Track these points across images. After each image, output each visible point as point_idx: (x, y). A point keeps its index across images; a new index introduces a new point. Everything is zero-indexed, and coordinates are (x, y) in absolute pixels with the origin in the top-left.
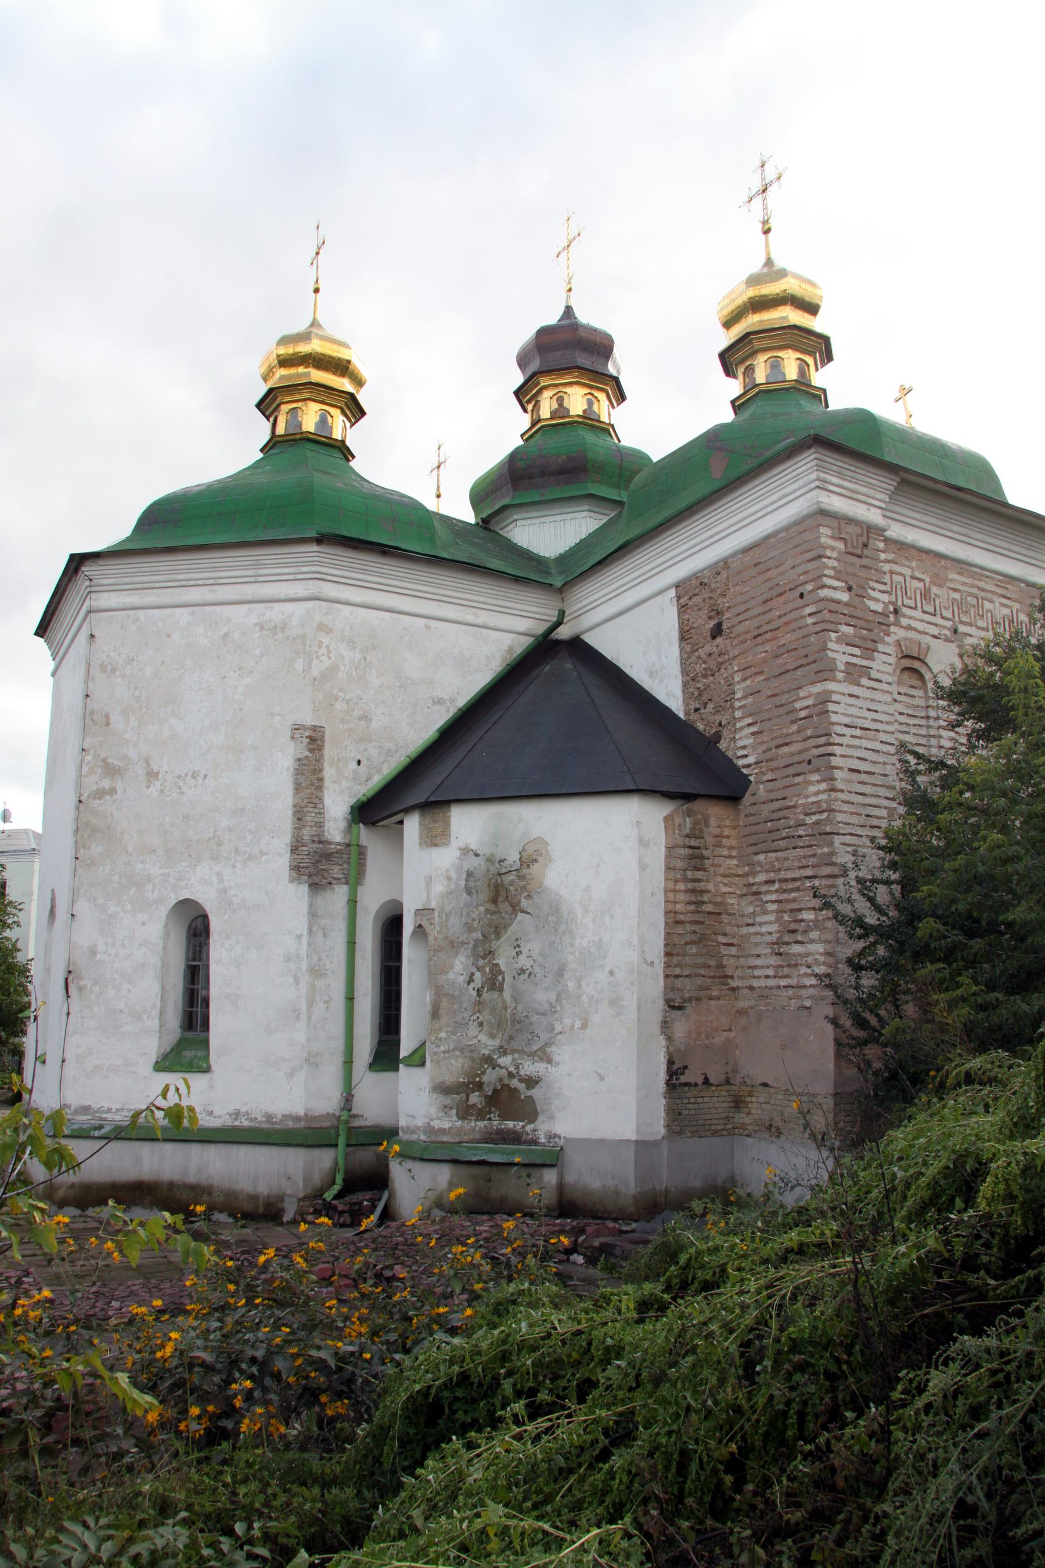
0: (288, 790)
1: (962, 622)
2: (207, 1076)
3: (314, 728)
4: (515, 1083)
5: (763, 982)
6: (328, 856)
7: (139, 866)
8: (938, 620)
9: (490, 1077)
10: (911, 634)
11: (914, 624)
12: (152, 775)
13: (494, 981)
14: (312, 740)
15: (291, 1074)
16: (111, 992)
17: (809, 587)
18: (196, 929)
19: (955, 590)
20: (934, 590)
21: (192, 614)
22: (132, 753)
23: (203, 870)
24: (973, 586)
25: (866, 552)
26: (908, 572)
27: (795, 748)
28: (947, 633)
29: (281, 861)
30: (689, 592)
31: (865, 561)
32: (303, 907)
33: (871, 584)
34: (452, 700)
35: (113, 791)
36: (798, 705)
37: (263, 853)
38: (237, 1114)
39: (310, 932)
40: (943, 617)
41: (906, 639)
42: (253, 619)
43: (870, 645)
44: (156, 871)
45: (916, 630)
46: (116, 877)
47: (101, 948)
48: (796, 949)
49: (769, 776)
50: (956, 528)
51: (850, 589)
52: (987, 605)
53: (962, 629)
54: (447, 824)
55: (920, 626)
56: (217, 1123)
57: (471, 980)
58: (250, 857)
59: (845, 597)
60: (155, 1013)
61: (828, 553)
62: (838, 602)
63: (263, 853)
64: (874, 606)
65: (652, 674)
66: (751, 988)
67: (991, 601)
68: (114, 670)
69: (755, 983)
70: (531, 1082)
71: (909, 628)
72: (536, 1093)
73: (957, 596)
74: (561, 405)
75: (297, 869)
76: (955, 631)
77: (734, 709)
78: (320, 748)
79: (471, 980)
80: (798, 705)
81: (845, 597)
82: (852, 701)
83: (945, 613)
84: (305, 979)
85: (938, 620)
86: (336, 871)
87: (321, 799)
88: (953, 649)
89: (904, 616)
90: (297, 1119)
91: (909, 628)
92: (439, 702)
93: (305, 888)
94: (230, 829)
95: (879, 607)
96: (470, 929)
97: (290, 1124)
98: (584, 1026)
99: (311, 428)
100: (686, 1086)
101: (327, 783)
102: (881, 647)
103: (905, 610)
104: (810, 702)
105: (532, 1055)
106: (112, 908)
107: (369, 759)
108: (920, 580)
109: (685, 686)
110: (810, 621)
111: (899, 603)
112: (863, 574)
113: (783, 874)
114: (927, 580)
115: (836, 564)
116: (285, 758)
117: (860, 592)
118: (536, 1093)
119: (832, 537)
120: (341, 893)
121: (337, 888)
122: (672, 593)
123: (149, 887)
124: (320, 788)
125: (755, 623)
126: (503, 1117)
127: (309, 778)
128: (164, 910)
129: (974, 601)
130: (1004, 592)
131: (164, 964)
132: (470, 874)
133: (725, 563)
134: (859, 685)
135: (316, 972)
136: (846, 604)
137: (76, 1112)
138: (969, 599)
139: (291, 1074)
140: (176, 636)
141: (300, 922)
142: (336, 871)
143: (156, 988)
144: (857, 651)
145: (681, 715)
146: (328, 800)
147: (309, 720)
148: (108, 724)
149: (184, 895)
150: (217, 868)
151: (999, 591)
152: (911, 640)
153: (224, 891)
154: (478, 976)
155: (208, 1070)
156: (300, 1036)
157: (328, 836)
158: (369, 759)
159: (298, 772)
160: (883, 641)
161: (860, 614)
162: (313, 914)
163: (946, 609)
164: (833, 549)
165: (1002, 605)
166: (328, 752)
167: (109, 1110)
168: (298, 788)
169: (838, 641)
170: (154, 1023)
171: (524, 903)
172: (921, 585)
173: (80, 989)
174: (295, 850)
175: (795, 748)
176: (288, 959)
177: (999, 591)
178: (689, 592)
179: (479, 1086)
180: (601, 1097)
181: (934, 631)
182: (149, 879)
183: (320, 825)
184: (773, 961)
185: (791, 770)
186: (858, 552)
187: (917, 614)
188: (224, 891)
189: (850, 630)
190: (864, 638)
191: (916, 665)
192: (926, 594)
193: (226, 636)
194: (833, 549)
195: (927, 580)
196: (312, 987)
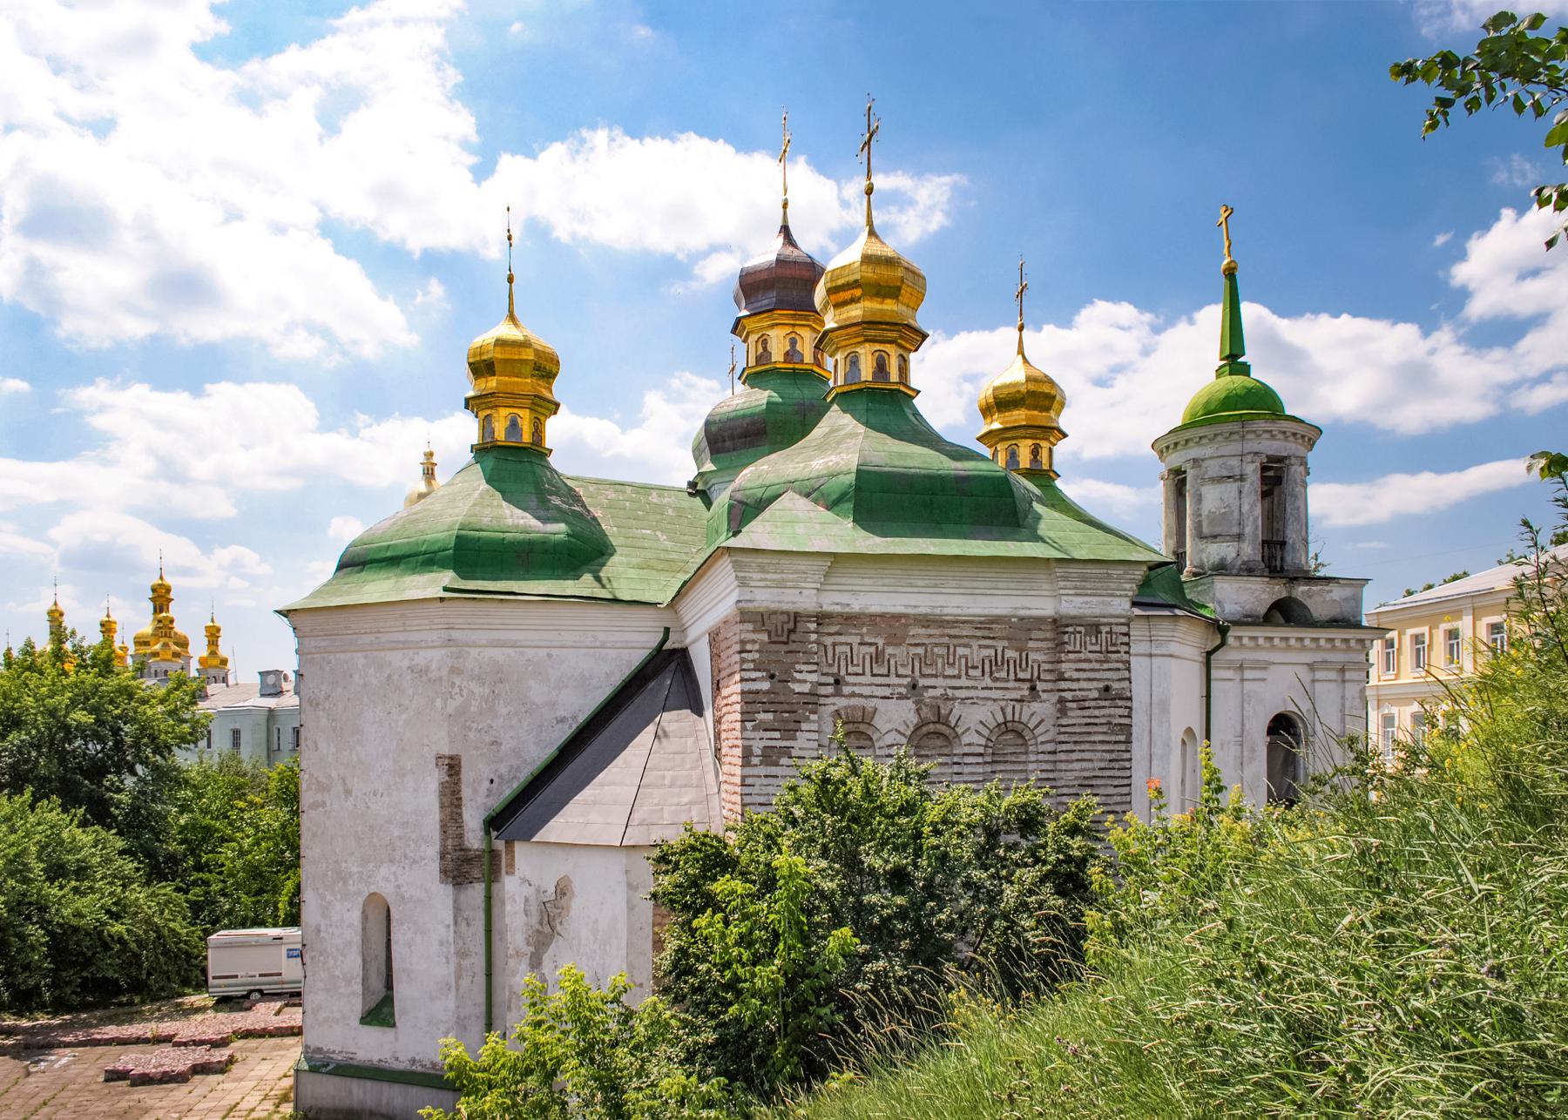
1: (923, 676)
3: (451, 758)
6: (468, 861)
8: (893, 680)
10: (854, 701)
11: (857, 690)
14: (451, 767)
16: (332, 962)
19: (917, 645)
20: (889, 650)
23: (384, 870)
24: (942, 636)
25: (793, 637)
26: (855, 640)
28: (903, 690)
29: (434, 867)
31: (793, 647)
32: (450, 903)
33: (798, 667)
34: (574, 718)
37: (422, 859)
38: (413, 1061)
39: (456, 923)
40: (898, 676)
41: (846, 708)
43: (792, 726)
44: (355, 870)
45: (861, 695)
50: (920, 583)
51: (772, 677)
52: (961, 651)
53: (922, 682)
55: (866, 691)
56: (401, 1066)
58: (414, 862)
59: (765, 686)
60: (359, 979)
61: (748, 647)
62: (757, 692)
63: (422, 859)
64: (797, 688)
67: (966, 646)
71: (853, 695)
73: (920, 650)
75: (444, 871)
76: (914, 687)
78: (458, 773)
81: (766, 686)
82: (771, 780)
83: (901, 671)
84: (453, 959)
85: (893, 680)
86: (476, 873)
87: (460, 815)
88: (910, 704)
89: (847, 684)
91: (853, 695)
92: (562, 720)
93: (450, 888)
94: (400, 838)
95: (806, 688)
96: (528, 944)
101: (465, 801)
102: (804, 726)
103: (849, 679)
106: (329, 898)
107: (501, 777)
108: (871, 644)
111: (843, 672)
112: (789, 659)
114: (881, 642)
115: (757, 656)
116: (433, 781)
117: (784, 677)
119: (754, 631)
120: (476, 892)
121: (476, 885)
124: (459, 806)
127: (451, 797)
128: (361, 900)
129: (943, 651)
130: (986, 633)
131: (365, 940)
132: (527, 900)
134: (777, 764)
135: (462, 954)
136: (767, 692)
138: (936, 650)
141: (448, 916)
142: (476, 873)
143: (359, 961)
144: (777, 735)
146: (466, 816)
147: (446, 752)
149: (373, 889)
150: (393, 869)
151: (979, 633)
152: (854, 708)
153: (399, 887)
155: (394, 1025)
156: (452, 1005)
157: (467, 844)
158: (501, 777)
159: (442, 794)
160: (807, 720)
161: (782, 699)
162: (457, 909)
163: (903, 666)
164: (754, 642)
165: (980, 647)
166: (466, 775)
168: (442, 807)
169: (755, 729)
170: (358, 988)
171: (559, 928)
172: (872, 649)
174: (442, 857)
176: (441, 944)
177: (979, 633)
181: (887, 692)
183: (461, 836)
186: (784, 639)
187: (868, 679)
188: (399, 887)
189: (770, 716)
190: (784, 721)
191: (862, 727)
192: (878, 657)
194: (754, 642)
195: (881, 642)
196: (460, 965)
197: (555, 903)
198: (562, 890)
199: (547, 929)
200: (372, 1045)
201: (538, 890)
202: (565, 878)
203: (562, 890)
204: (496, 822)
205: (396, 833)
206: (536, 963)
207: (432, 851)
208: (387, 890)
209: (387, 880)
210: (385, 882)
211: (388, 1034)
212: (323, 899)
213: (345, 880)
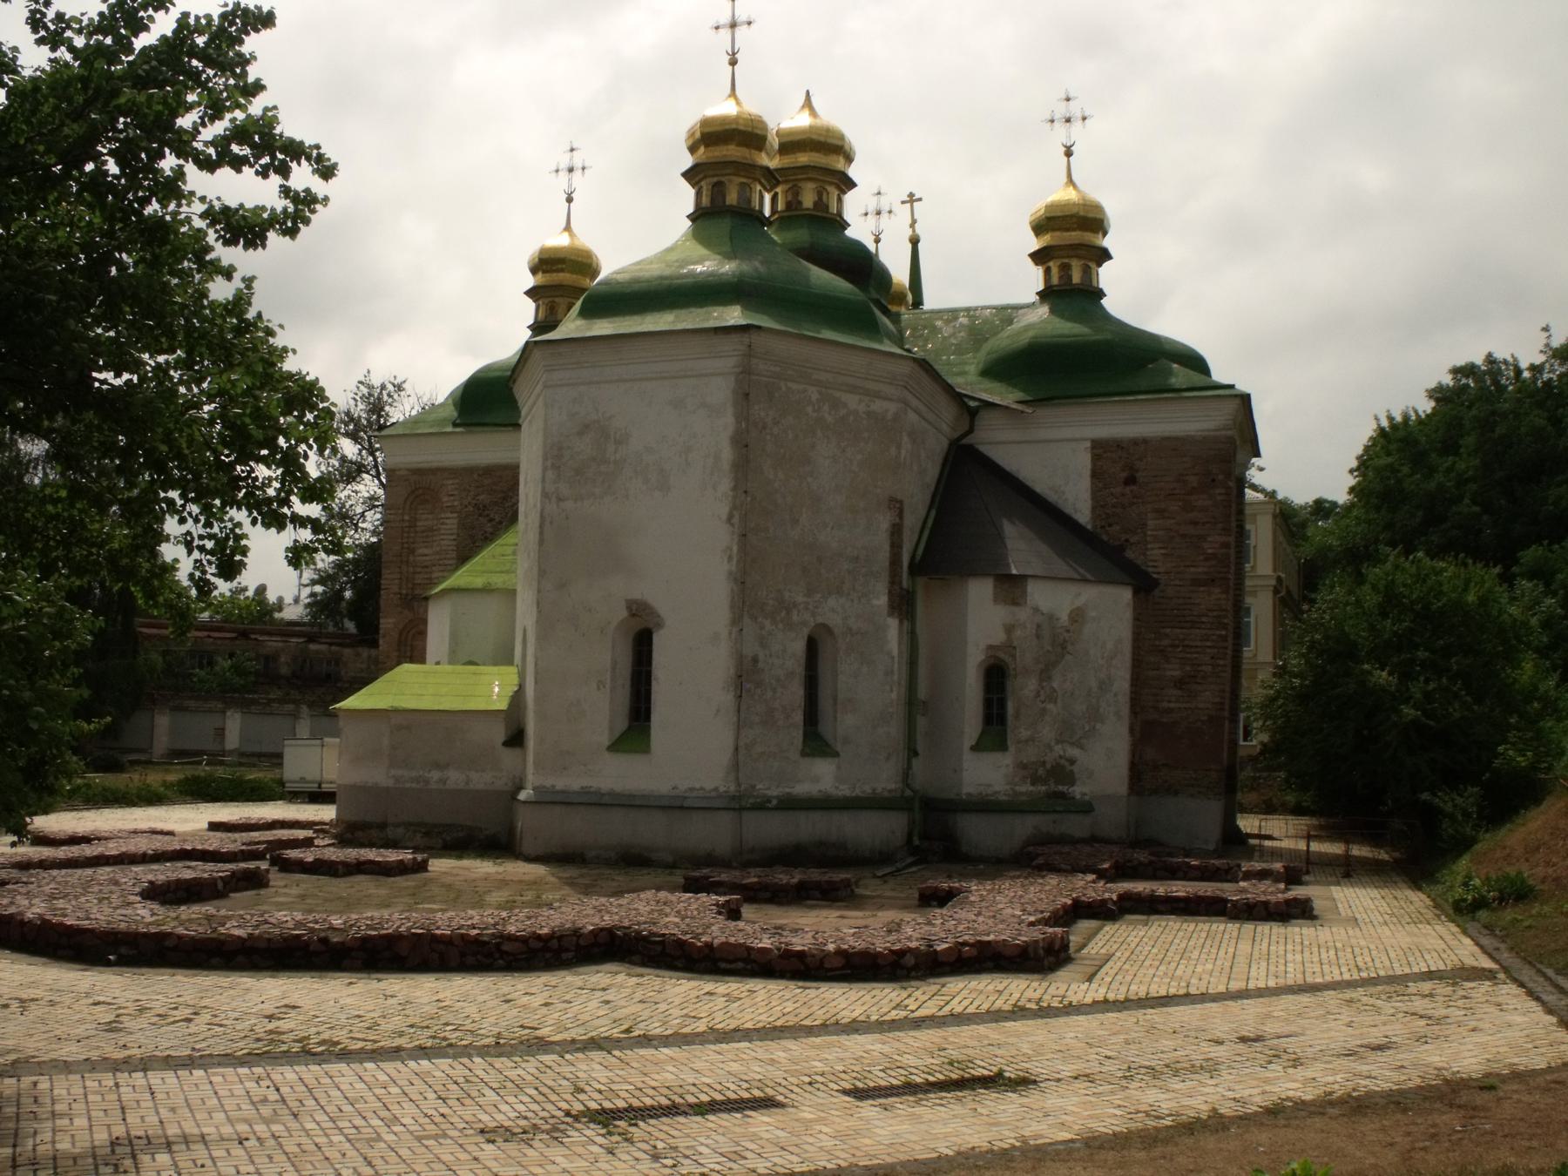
0: (887, 547)
2: (836, 760)
4: (1063, 761)
7: (787, 594)
15: (888, 759)
16: (769, 694)
23: (832, 602)
30: (1101, 450)
44: (800, 599)
47: (761, 657)
54: (1025, 592)
57: (1038, 695)
68: (764, 428)
70: (1072, 762)
74: (820, 198)
97: (886, 794)
99: (735, 203)
105: (1072, 744)
109: (1094, 509)
116: (884, 522)
118: (1075, 768)
122: (1088, 444)
123: (795, 612)
126: (1057, 783)
128: (806, 631)
132: (1039, 626)
133: (1145, 441)
139: (888, 759)
143: (802, 692)
145: (1089, 527)
149: (820, 620)
173: (749, 691)
178: (1101, 450)
182: (795, 605)
204: (916, 569)
206: (1045, 674)
208: (835, 621)
209: (833, 610)
210: (834, 612)
212: (762, 628)
213: (789, 612)
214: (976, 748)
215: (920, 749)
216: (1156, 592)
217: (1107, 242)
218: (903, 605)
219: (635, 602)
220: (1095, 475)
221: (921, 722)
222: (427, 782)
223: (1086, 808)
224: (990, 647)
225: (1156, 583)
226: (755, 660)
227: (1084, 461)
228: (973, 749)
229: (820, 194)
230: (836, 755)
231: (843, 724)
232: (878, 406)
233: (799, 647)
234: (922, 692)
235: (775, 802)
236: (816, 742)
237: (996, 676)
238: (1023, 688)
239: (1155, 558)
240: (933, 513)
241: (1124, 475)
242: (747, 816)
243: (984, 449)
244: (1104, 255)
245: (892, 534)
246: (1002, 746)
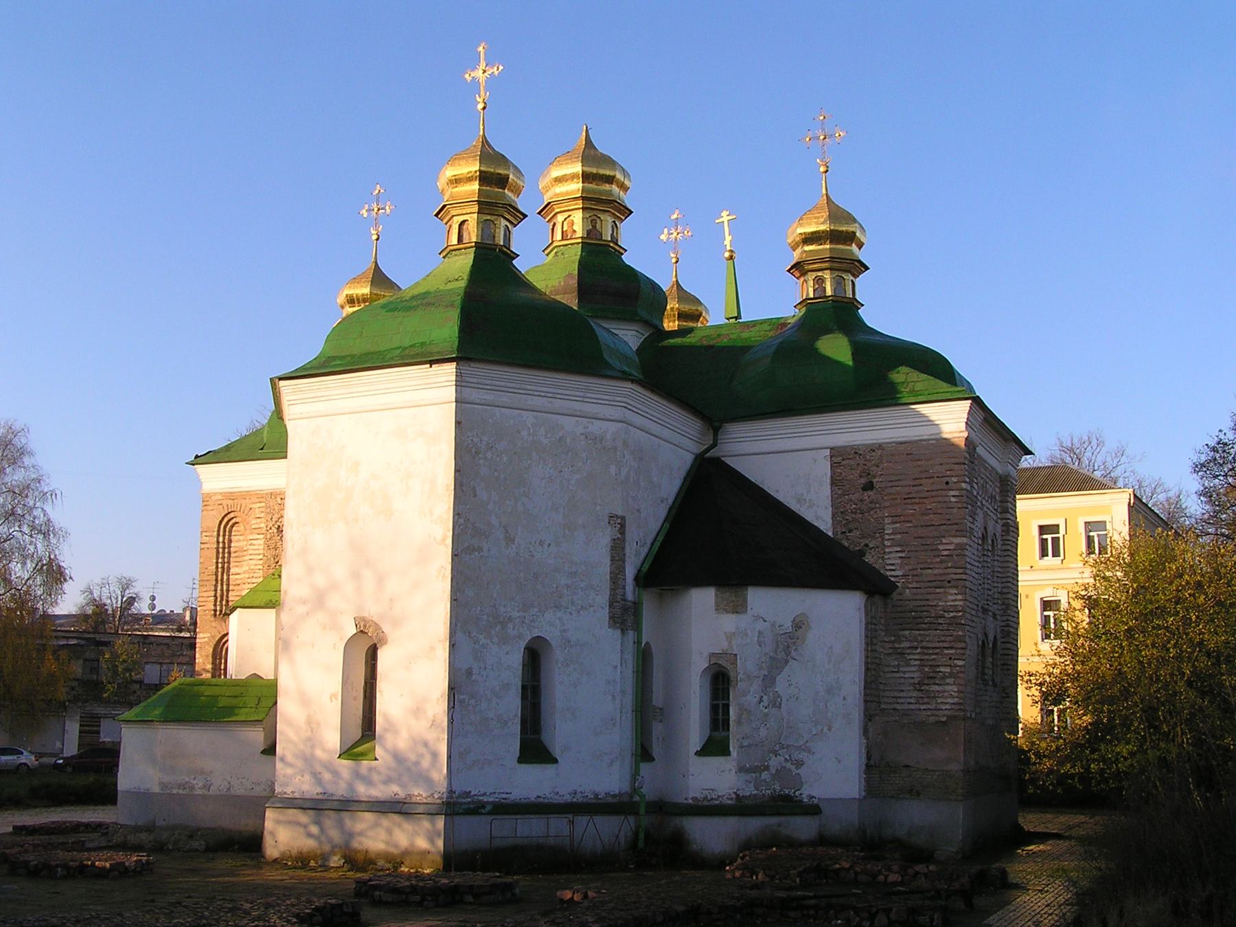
4: (789, 765)
5: (906, 707)
7: (502, 609)
9: (774, 762)
12: (510, 540)
13: (776, 703)
17: (955, 480)
18: (534, 656)
21: (536, 417)
22: (494, 521)
23: (549, 615)
27: (936, 572)
29: (604, 614)
35: (480, 549)
36: (941, 547)
42: (580, 430)
46: (485, 617)
48: (936, 688)
49: (914, 585)
54: (745, 601)
57: (761, 700)
65: (799, 501)
66: (895, 709)
69: (898, 707)
72: (801, 771)
74: (594, 227)
77: (883, 539)
79: (761, 700)
80: (941, 547)
90: (614, 796)
96: (760, 668)
97: (610, 800)
98: (830, 730)
100: (878, 769)
104: (952, 547)
106: (483, 641)
110: (953, 499)
113: (924, 644)
116: (605, 538)
122: (828, 452)
123: (510, 626)
125: (907, 490)
132: (760, 633)
137: (459, 796)
140: (524, 433)
143: (519, 702)
145: (830, 534)
147: (620, 513)
148: (475, 496)
150: (559, 614)
154: (765, 698)
155: (555, 761)
167: (484, 794)
171: (793, 654)
173: (462, 702)
175: (936, 572)
178: (839, 456)
179: (767, 768)
180: (834, 772)
184: (915, 694)
185: (934, 584)
193: (561, 439)
197: (790, 635)
198: (799, 624)
199: (781, 655)
200: (532, 783)
201: (773, 625)
202: (803, 614)
203: (799, 624)
205: (563, 581)
206: (769, 681)
207: (602, 599)
210: (548, 627)
211: (549, 769)
214: (698, 753)
215: (656, 750)
216: (895, 595)
217: (862, 255)
218: (625, 616)
219: (363, 619)
220: (834, 482)
221: (657, 729)
222: (192, 788)
223: (813, 810)
224: (712, 655)
225: (894, 586)
226: (469, 672)
227: (824, 469)
228: (698, 753)
229: (593, 223)
230: (555, 761)
231: (561, 732)
232: (596, 427)
233: (516, 658)
234: (658, 698)
235: (489, 808)
236: (534, 750)
237: (720, 681)
238: (743, 697)
239: (892, 564)
240: (667, 525)
241: (863, 481)
242: (457, 818)
243: (729, 461)
244: (859, 267)
245: (613, 548)
246: (725, 752)
